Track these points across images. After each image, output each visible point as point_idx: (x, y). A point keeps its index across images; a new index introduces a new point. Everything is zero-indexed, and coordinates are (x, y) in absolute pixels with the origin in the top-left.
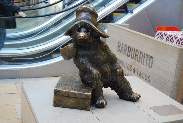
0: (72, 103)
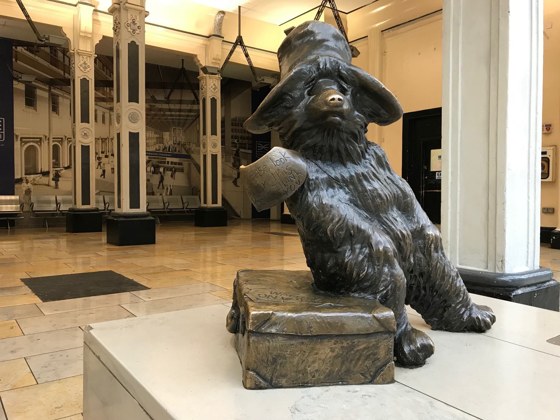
0: (324, 360)
